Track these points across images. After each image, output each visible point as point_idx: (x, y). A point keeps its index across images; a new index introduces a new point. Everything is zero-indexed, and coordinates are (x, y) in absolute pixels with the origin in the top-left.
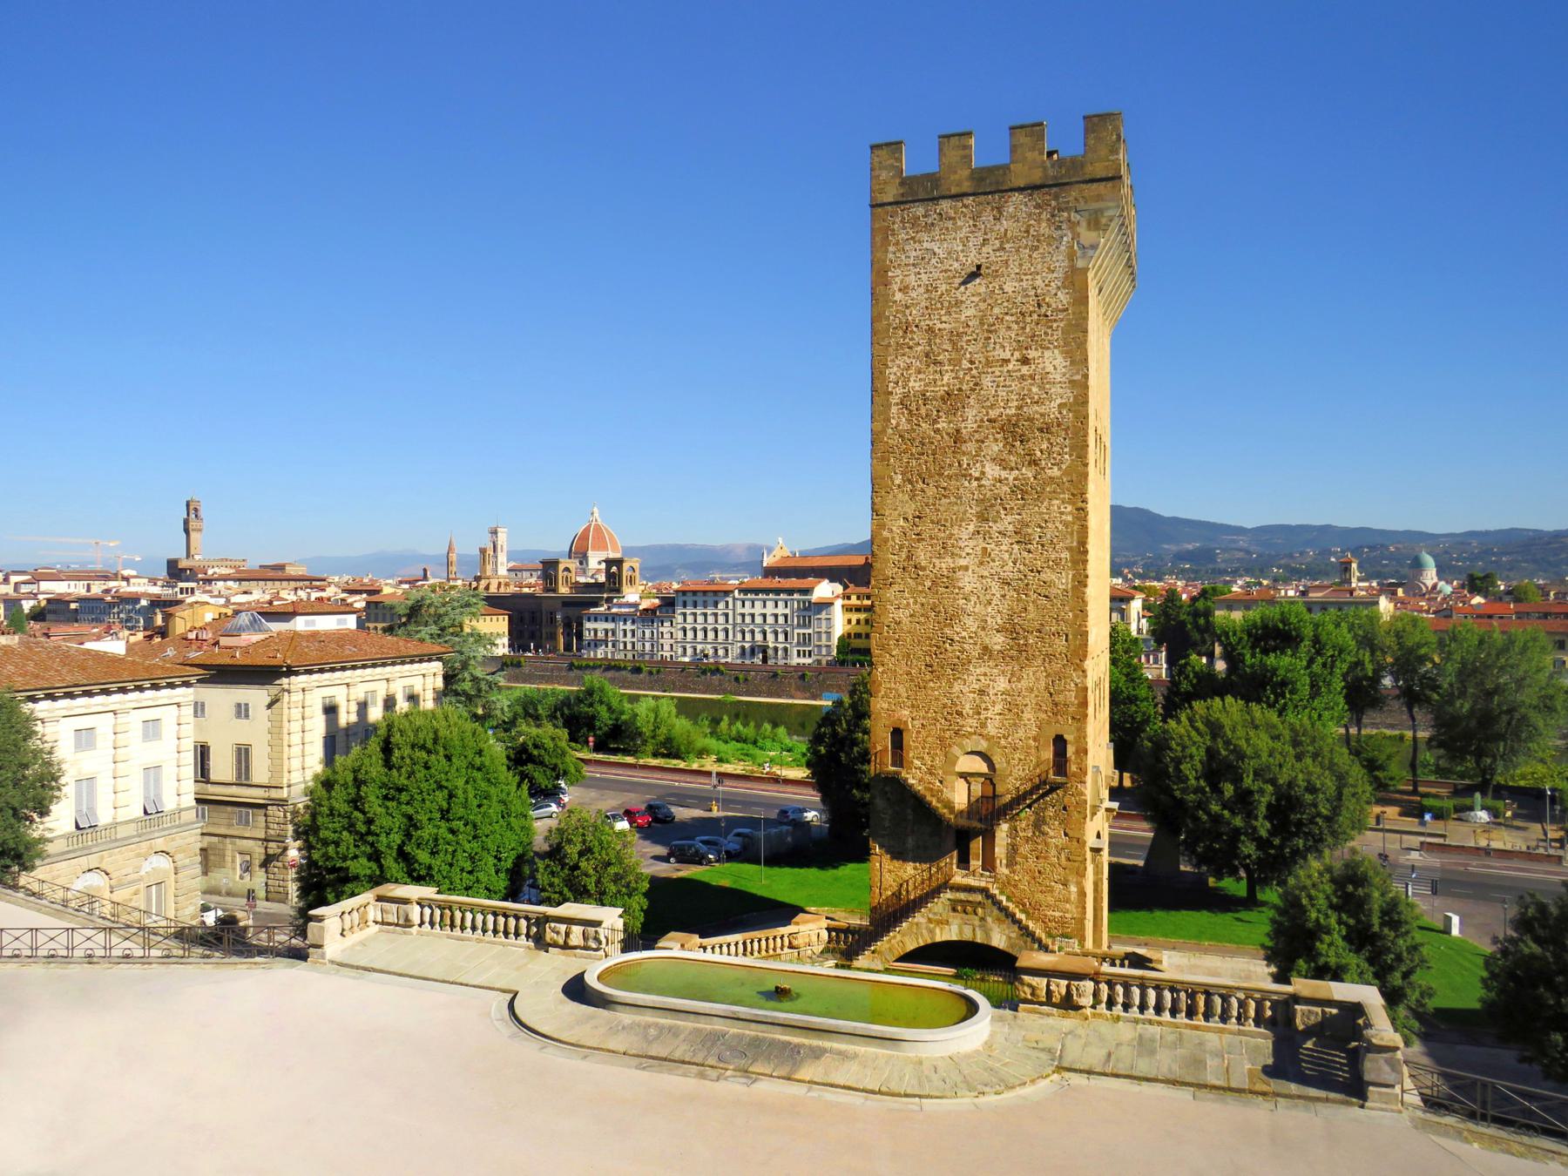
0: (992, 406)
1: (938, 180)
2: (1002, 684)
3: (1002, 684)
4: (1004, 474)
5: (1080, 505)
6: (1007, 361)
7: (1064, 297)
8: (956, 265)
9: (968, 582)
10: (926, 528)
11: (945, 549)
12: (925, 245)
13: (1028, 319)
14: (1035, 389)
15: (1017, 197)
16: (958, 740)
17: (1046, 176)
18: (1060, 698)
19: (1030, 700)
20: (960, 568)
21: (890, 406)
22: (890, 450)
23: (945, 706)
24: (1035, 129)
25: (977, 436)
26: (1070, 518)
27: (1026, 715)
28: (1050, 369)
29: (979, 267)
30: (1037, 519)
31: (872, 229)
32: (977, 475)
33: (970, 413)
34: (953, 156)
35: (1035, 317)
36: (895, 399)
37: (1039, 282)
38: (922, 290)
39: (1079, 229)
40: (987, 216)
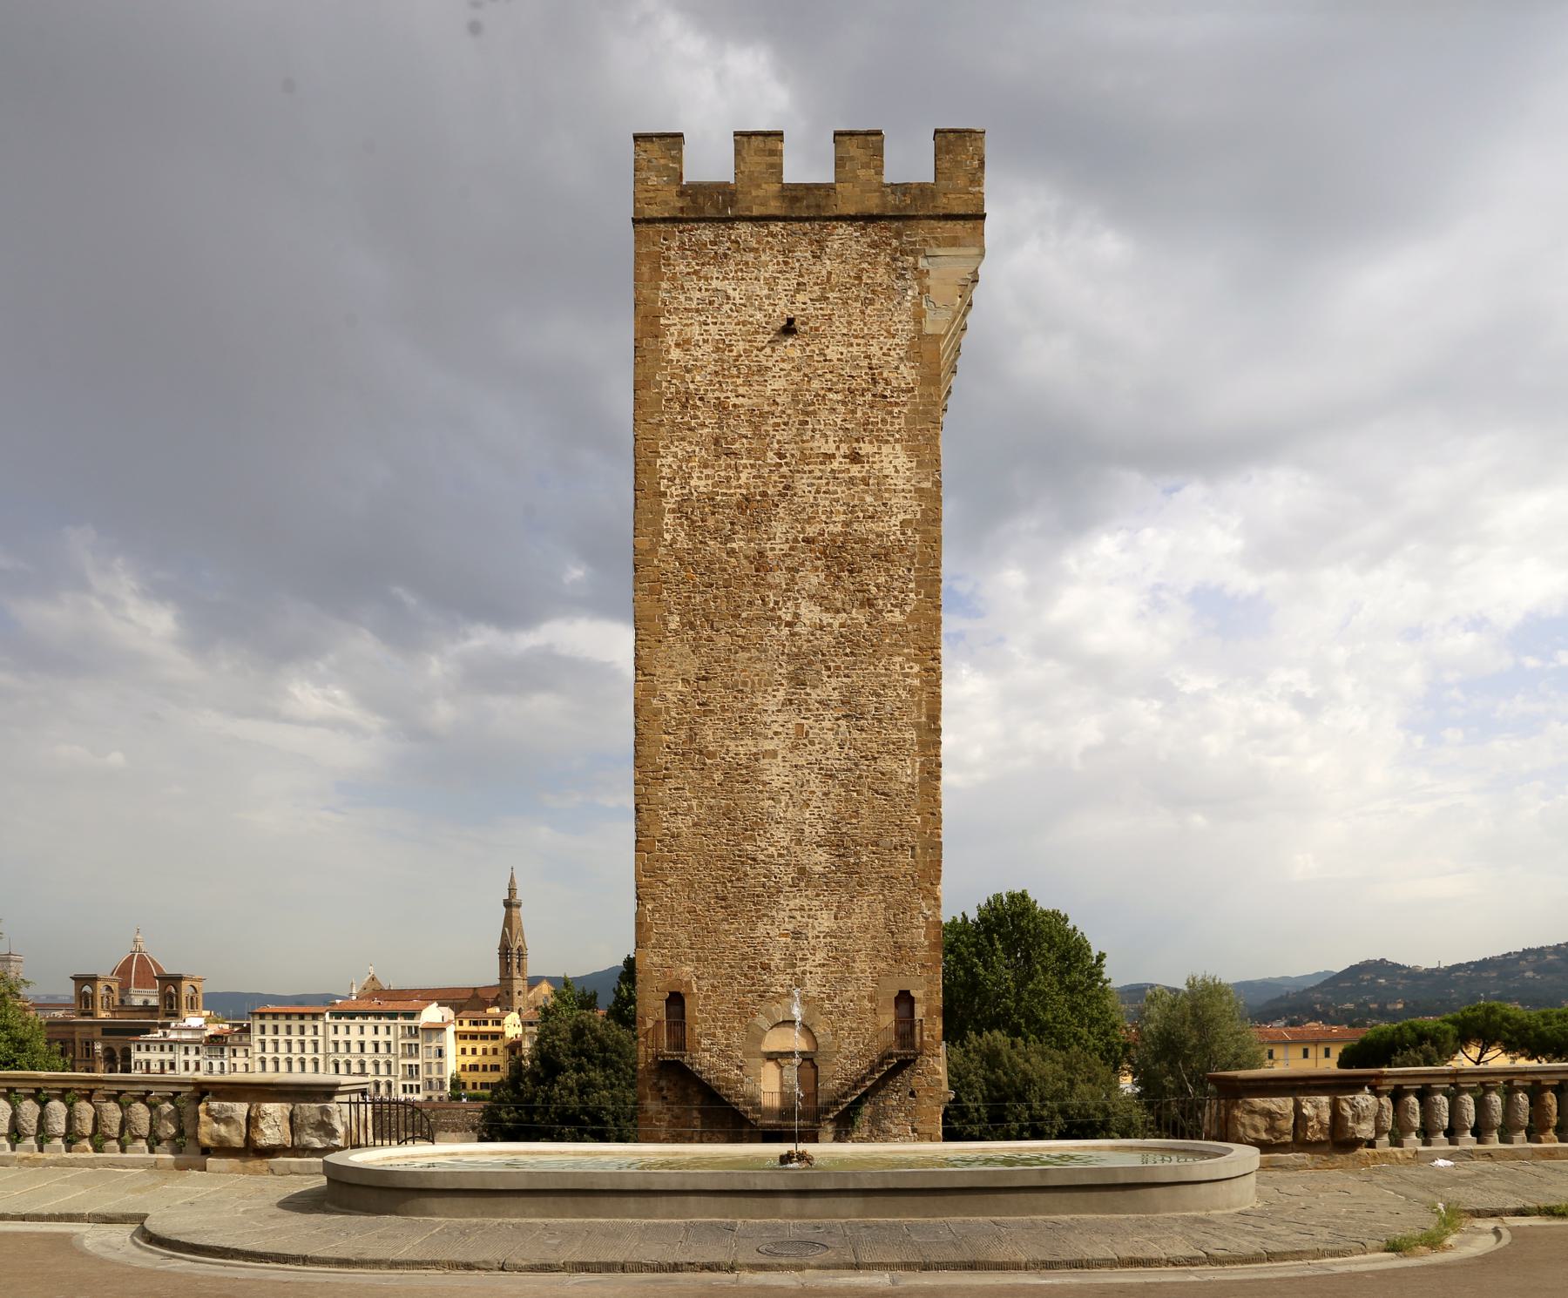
0: (809, 520)
1: (733, 194)
2: (825, 921)
3: (825, 921)
4: (827, 618)
5: (931, 664)
6: (833, 456)
7: (908, 373)
8: (759, 315)
9: (776, 773)
10: (716, 694)
11: (746, 726)
12: (715, 284)
13: (860, 400)
14: (869, 499)
15: (844, 230)
16: (765, 1006)
17: (884, 205)
18: (905, 939)
19: (865, 943)
20: (766, 754)
21: (661, 513)
22: (661, 580)
23: (744, 957)
24: (871, 140)
25: (788, 562)
26: (916, 682)
27: (858, 966)
28: (890, 471)
29: (791, 321)
30: (873, 684)
31: (637, 255)
32: (789, 618)
33: (779, 528)
34: (756, 162)
35: (869, 397)
36: (669, 504)
37: (874, 350)
38: (708, 348)
39: (928, 282)
40: (803, 252)
